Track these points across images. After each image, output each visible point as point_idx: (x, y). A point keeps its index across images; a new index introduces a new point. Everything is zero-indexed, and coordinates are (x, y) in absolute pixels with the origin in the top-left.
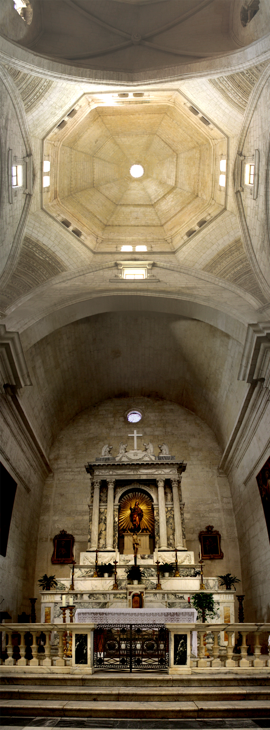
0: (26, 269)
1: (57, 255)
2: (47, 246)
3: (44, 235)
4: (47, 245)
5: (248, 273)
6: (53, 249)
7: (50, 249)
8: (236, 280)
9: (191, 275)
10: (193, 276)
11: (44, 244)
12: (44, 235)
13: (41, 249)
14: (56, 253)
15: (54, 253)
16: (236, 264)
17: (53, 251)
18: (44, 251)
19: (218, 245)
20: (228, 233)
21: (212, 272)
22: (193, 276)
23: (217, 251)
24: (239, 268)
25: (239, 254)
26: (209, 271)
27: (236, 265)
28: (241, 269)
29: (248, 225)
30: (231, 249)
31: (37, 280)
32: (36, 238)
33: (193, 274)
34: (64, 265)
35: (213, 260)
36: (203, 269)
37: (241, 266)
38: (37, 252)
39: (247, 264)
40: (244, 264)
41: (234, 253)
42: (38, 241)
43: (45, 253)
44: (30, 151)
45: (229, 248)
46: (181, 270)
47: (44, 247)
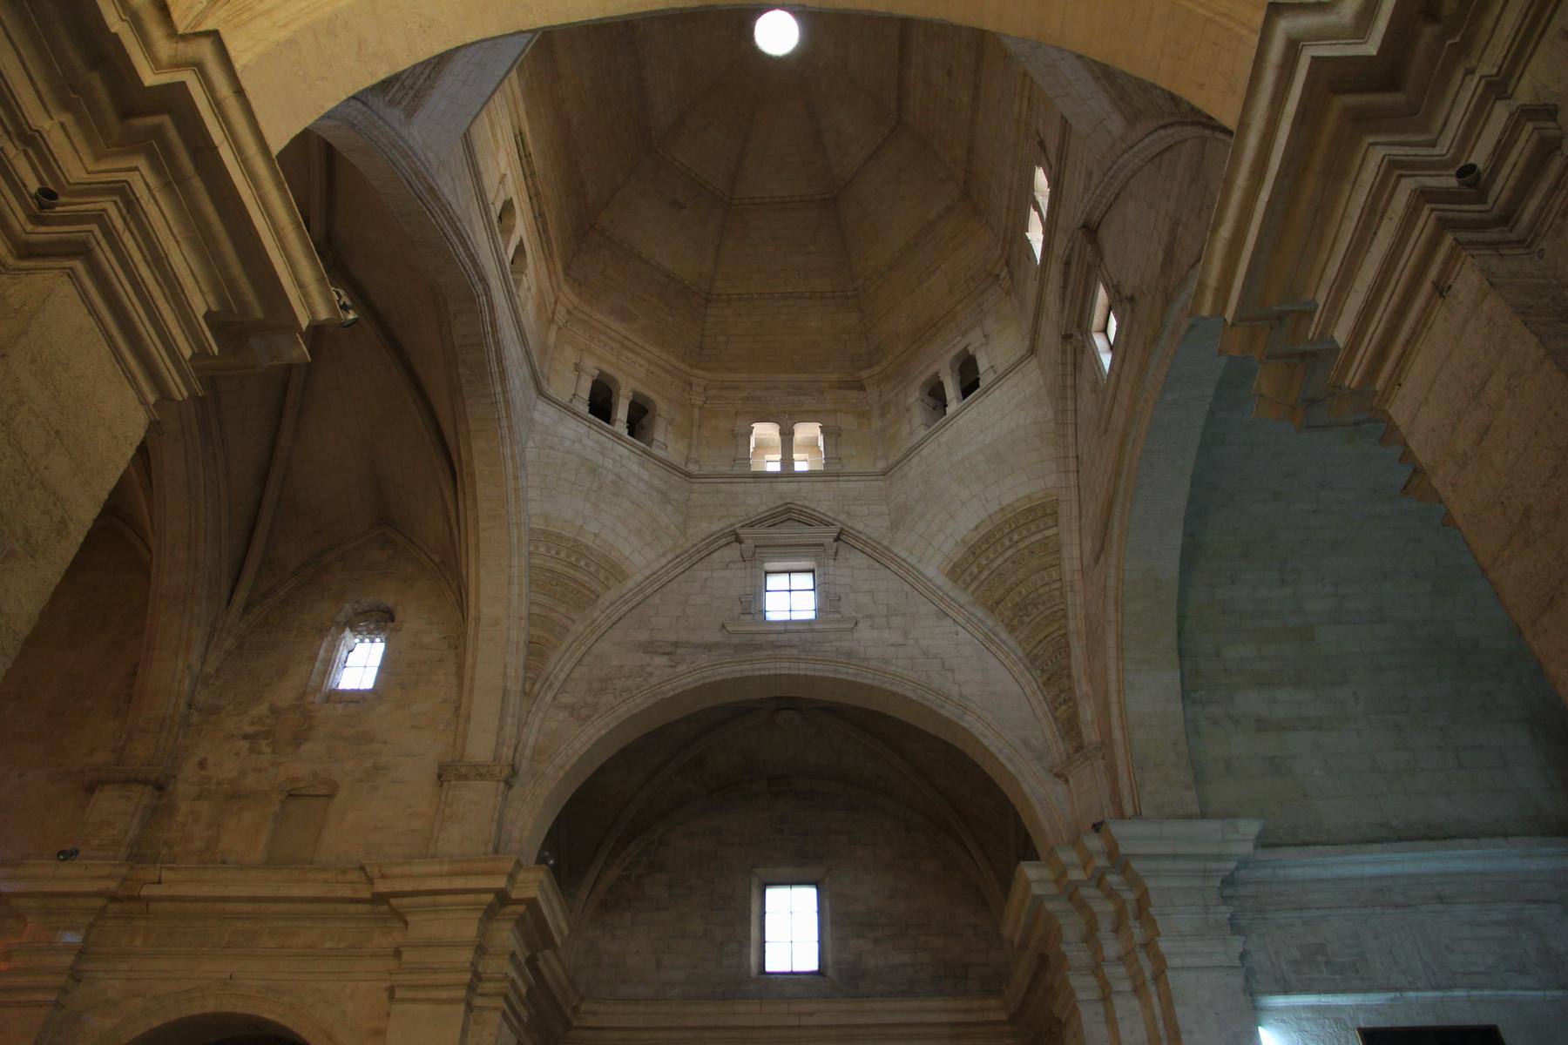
0: (1025, 619)
1: (1010, 505)
2: (982, 522)
3: (952, 517)
4: (980, 520)
6: (993, 507)
7: (990, 516)
11: (976, 527)
12: (952, 517)
13: (987, 541)
14: (1005, 503)
15: (1003, 509)
17: (997, 508)
18: (994, 536)
31: (1056, 608)
32: (957, 543)
34: (1041, 498)
38: (992, 556)
42: (964, 541)
43: (998, 536)
44: (725, 537)
47: (983, 531)
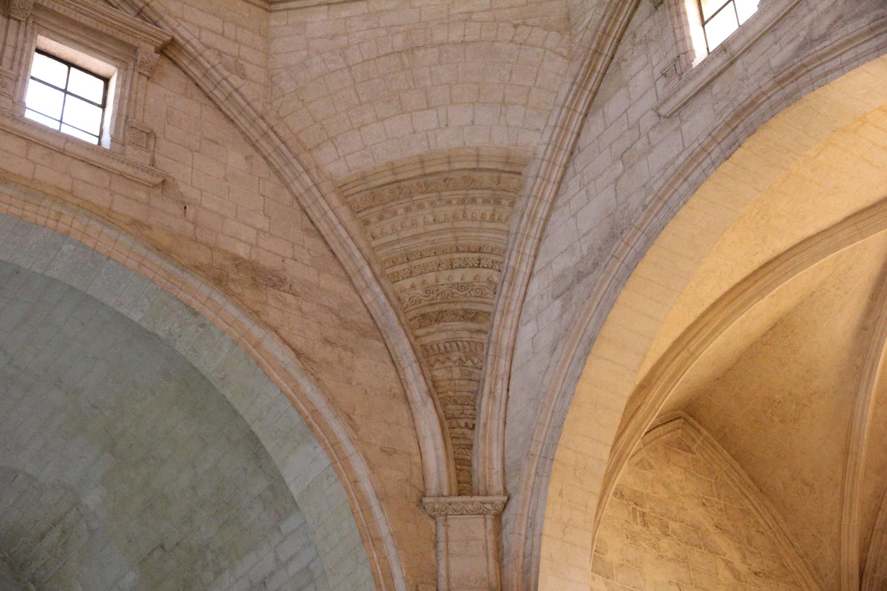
5: (473, 320)
8: (425, 319)
9: (288, 186)
10: (292, 193)
16: (458, 251)
19: (443, 125)
20: (503, 103)
21: (367, 223)
22: (292, 193)
23: (425, 143)
24: (457, 276)
25: (488, 217)
26: (355, 211)
27: (456, 256)
28: (461, 287)
29: (582, 142)
30: (477, 175)
33: (297, 188)
35: (393, 167)
36: (340, 188)
37: (469, 275)
39: (490, 281)
40: (484, 273)
41: (474, 200)
45: (473, 165)
46: (263, 143)
